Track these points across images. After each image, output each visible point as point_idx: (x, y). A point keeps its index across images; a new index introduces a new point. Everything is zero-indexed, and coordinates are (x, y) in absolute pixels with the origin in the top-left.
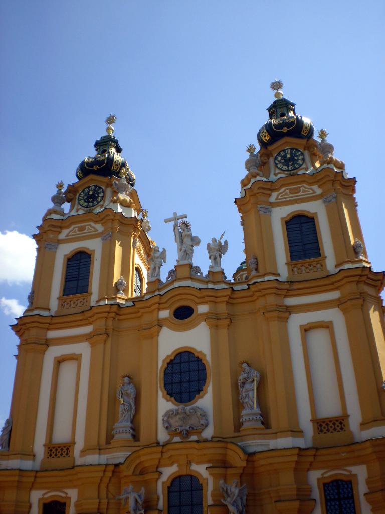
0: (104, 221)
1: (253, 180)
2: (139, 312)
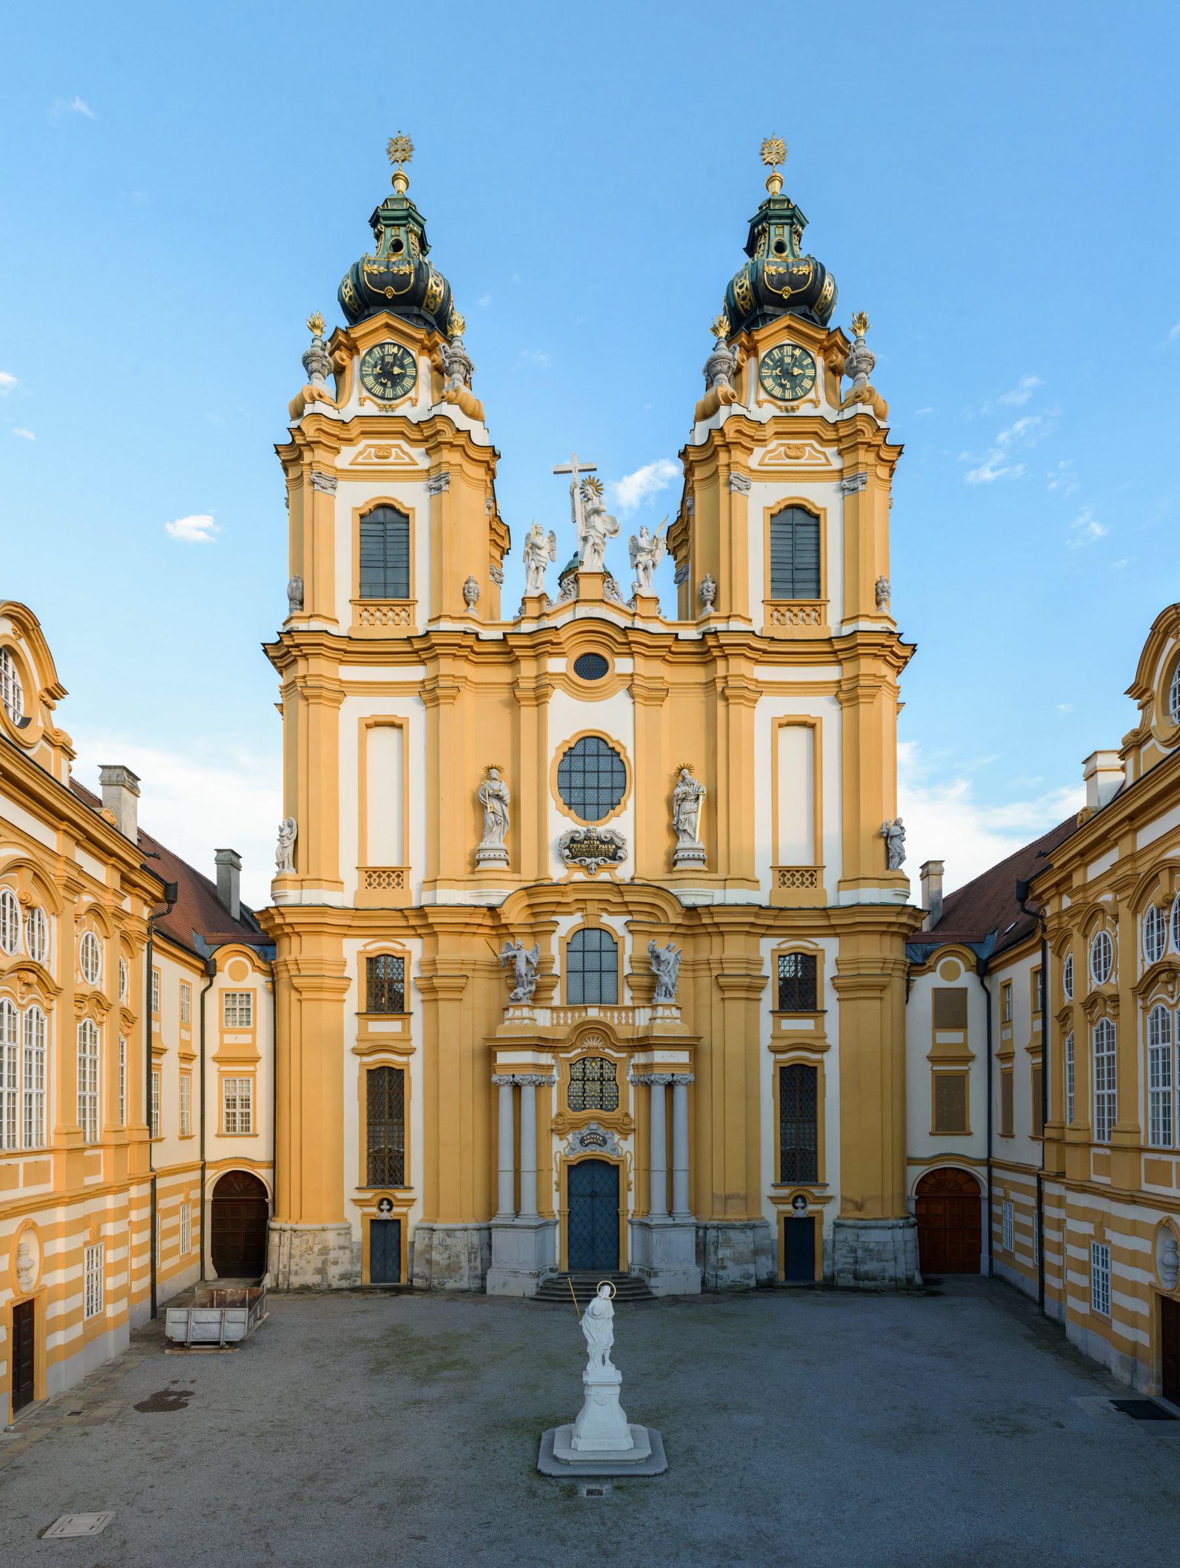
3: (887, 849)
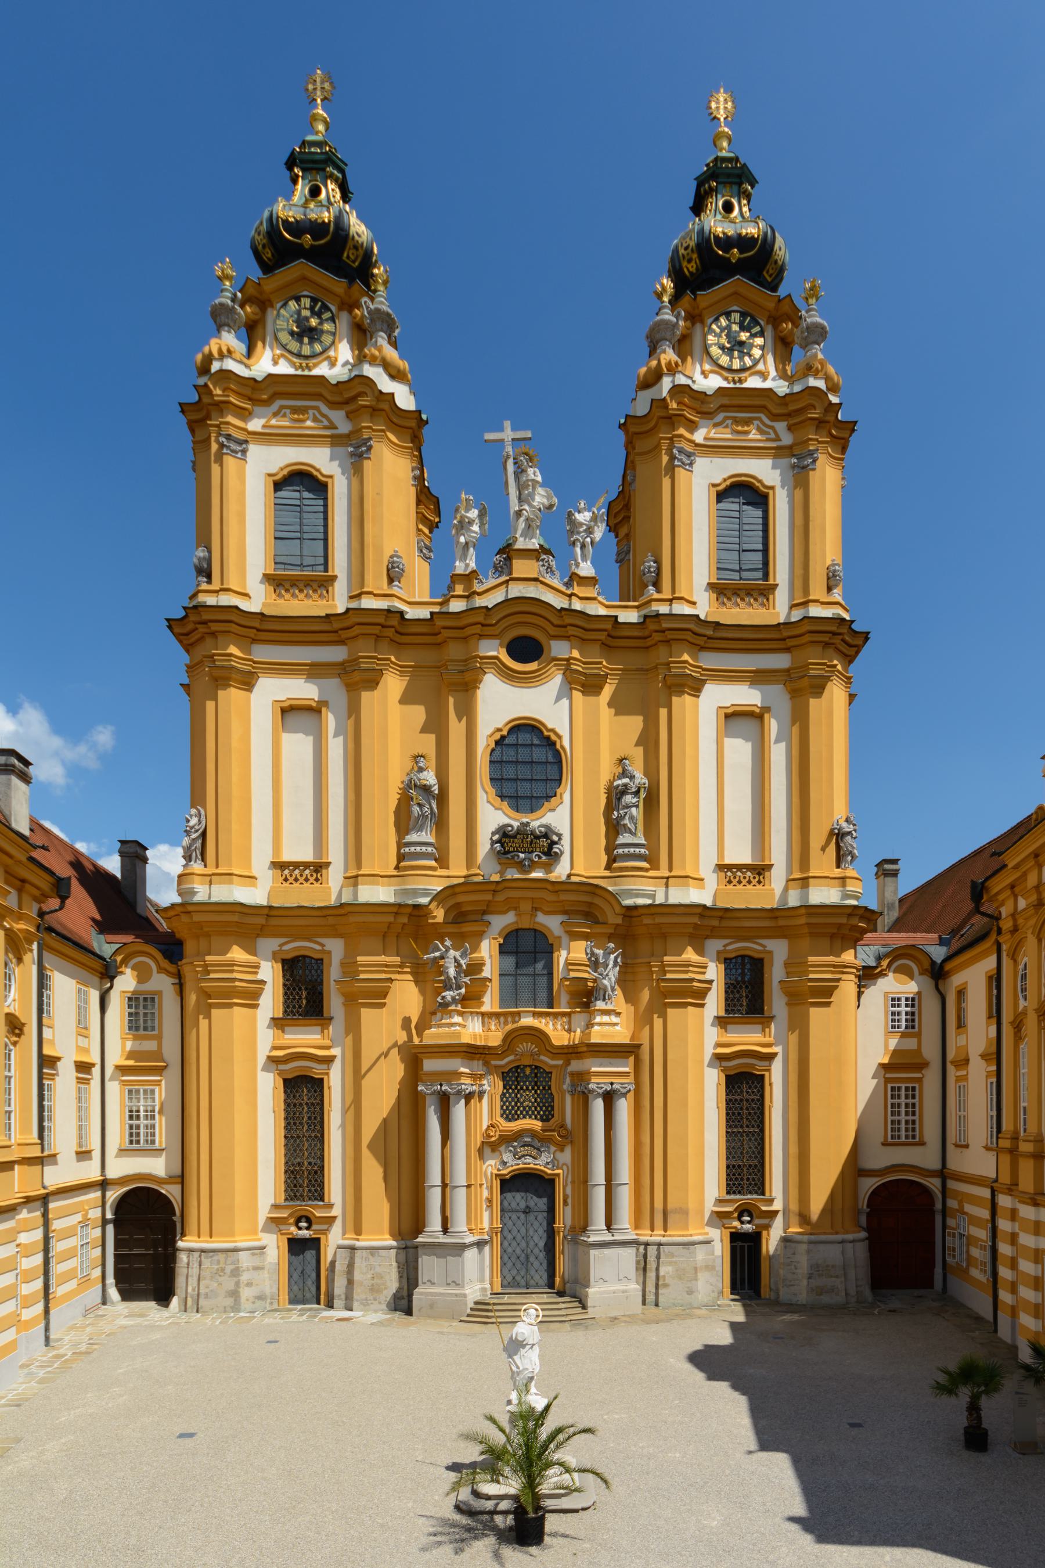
0: (352, 407)
1: (667, 383)
2: (440, 633)
3: (838, 848)
